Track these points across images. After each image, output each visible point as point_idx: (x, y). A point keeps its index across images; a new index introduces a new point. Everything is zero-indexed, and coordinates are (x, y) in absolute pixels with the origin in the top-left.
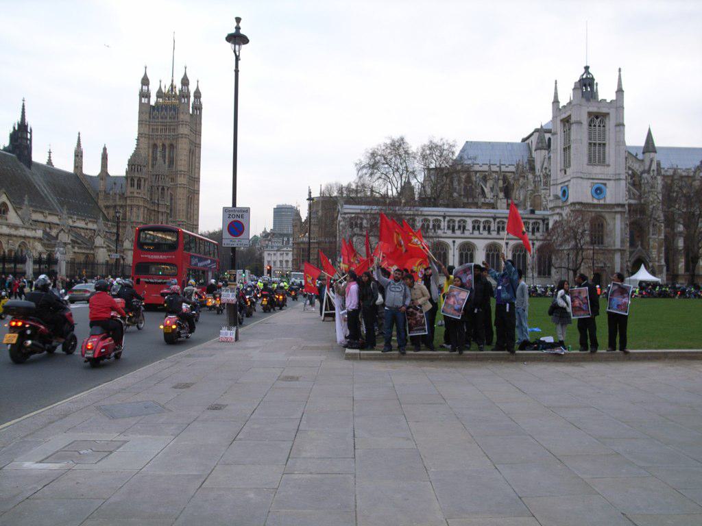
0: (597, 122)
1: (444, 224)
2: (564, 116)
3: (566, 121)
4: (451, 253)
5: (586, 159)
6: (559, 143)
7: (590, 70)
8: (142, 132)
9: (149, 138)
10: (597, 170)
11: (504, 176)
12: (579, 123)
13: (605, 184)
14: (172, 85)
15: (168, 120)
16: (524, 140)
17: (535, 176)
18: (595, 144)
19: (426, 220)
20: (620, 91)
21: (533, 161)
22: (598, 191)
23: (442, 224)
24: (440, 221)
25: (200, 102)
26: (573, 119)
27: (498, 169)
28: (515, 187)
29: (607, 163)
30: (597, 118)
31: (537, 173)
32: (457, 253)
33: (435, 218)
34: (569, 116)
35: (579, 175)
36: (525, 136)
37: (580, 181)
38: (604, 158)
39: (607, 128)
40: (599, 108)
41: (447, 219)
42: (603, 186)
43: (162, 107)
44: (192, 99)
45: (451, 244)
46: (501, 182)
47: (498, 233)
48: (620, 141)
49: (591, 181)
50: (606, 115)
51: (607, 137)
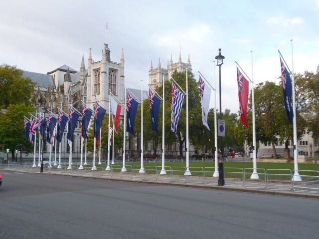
0: (112, 73)
3: (97, 71)
6: (92, 80)
7: (108, 46)
11: (41, 93)
12: (105, 73)
16: (49, 73)
17: (64, 96)
18: (111, 84)
20: (123, 60)
21: (63, 87)
26: (101, 70)
27: (37, 89)
28: (48, 100)
30: (113, 71)
31: (65, 94)
34: (99, 68)
36: (50, 71)
39: (117, 77)
40: (114, 66)
46: (39, 96)
48: (123, 85)
50: (116, 71)
51: (117, 82)
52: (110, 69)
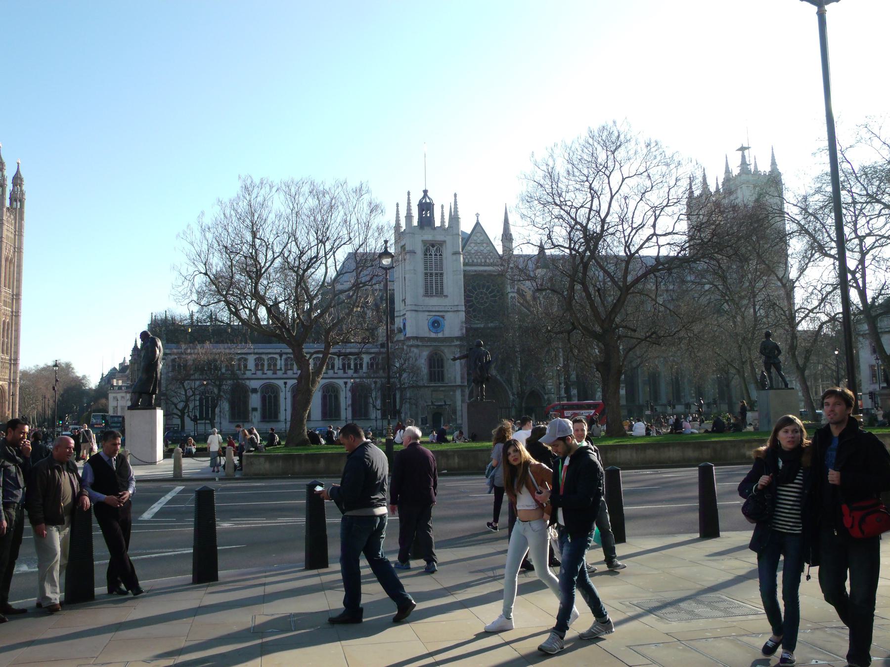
0: (433, 250)
2: (403, 243)
4: (282, 395)
5: (421, 291)
7: (428, 194)
10: (434, 302)
12: (413, 252)
13: (443, 317)
18: (431, 274)
22: (436, 324)
23: (279, 362)
24: (276, 359)
25: (21, 191)
29: (445, 294)
30: (433, 246)
32: (289, 395)
33: (270, 356)
35: (416, 308)
37: (414, 314)
38: (442, 288)
39: (444, 255)
41: (284, 357)
42: (441, 319)
44: (9, 187)
45: (283, 386)
47: (345, 372)
49: (427, 313)
50: (442, 243)
52: (424, 242)
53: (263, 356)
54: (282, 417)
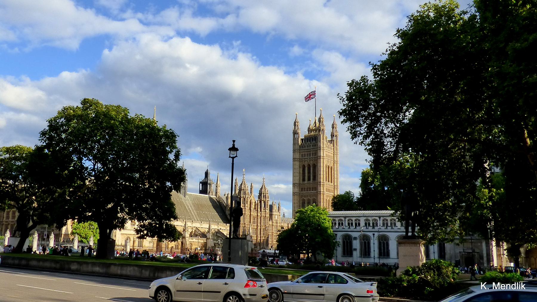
1: (380, 222)
4: (372, 242)
8: (295, 157)
9: (300, 161)
14: (315, 122)
15: (311, 147)
19: (367, 220)
23: (378, 222)
41: (382, 218)
43: (313, 138)
45: (372, 236)
53: (369, 218)
54: (372, 255)
